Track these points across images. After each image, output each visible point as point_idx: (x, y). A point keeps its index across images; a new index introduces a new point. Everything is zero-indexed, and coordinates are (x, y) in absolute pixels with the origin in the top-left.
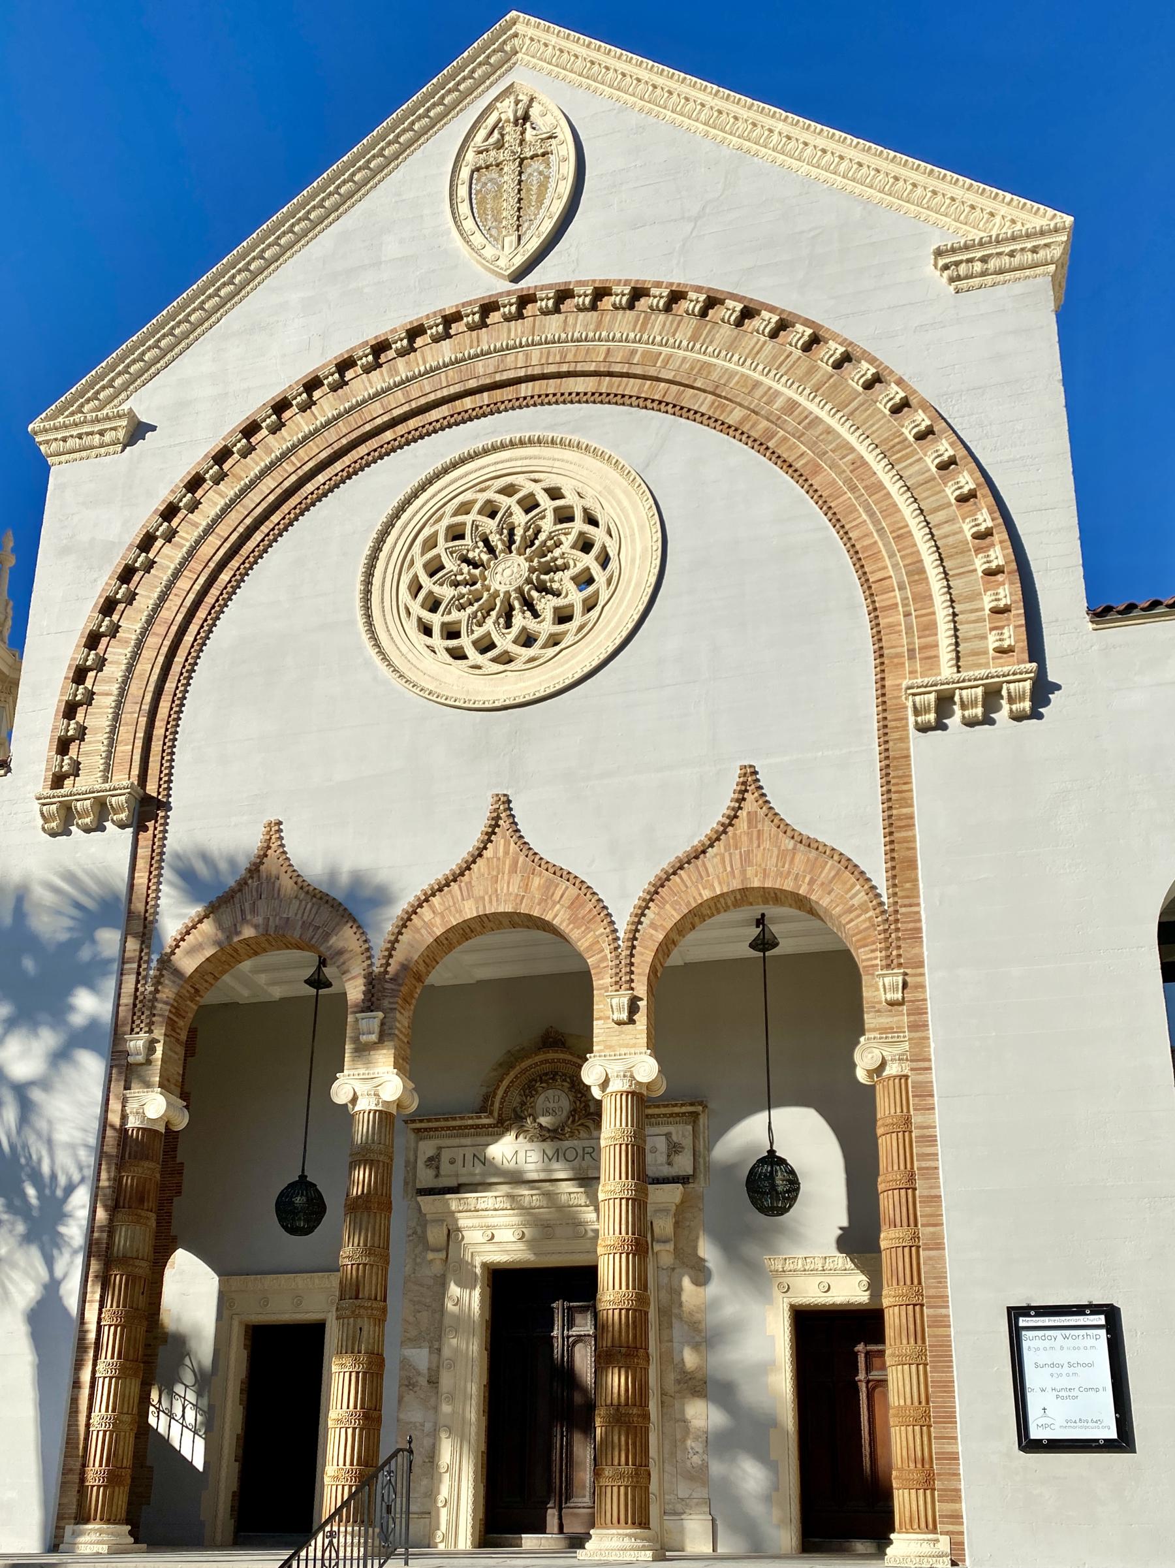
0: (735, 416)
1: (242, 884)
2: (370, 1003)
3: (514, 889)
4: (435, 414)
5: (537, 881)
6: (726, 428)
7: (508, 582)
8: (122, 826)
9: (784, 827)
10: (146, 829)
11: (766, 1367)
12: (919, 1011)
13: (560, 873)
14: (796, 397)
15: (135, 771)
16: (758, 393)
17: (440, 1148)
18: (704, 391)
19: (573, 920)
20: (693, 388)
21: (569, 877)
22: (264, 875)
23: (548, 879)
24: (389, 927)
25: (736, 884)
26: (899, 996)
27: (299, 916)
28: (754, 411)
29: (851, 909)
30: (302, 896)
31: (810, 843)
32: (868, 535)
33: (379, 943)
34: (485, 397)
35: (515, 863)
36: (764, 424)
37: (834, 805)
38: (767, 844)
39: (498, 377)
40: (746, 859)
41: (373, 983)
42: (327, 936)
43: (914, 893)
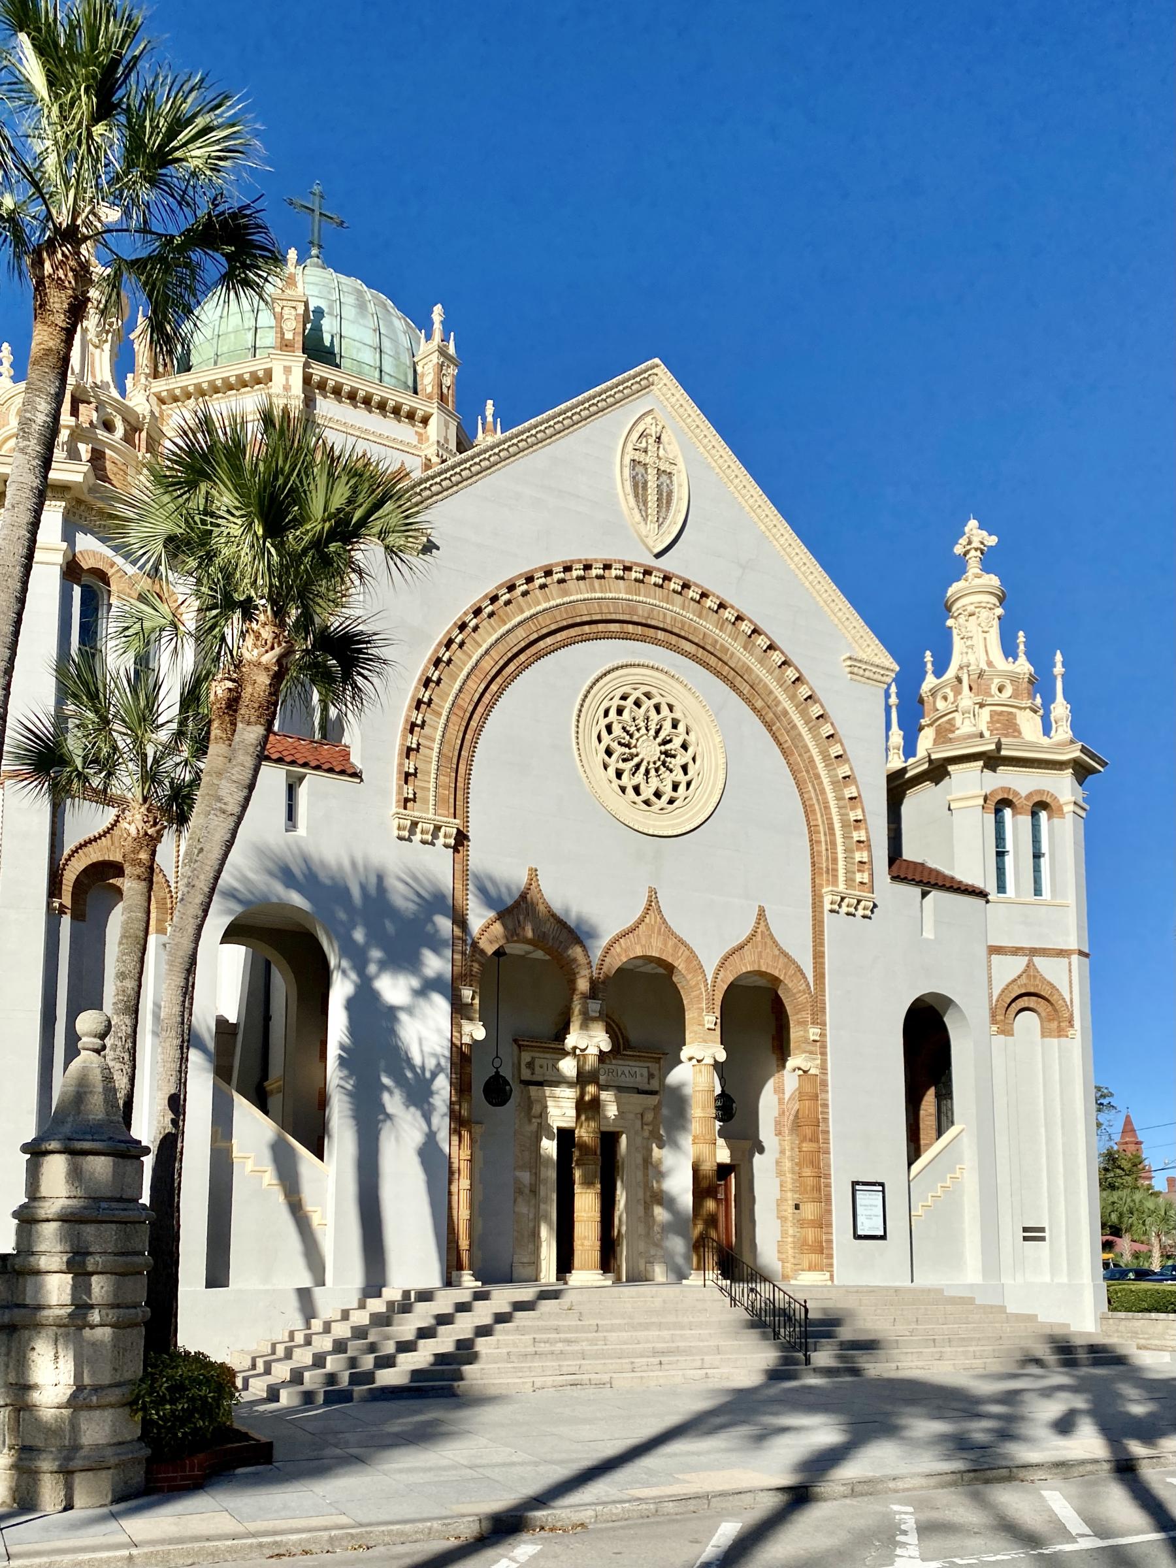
1: (517, 904)
2: (594, 992)
3: (660, 945)
5: (670, 943)
6: (754, 709)
7: (644, 755)
8: (446, 846)
9: (775, 942)
10: (458, 852)
12: (824, 1046)
13: (681, 941)
16: (772, 697)
17: (533, 1058)
19: (687, 969)
21: (687, 946)
25: (756, 968)
29: (800, 991)
31: (786, 955)
32: (811, 799)
40: (760, 956)
41: (593, 983)
42: (567, 948)
43: (823, 990)
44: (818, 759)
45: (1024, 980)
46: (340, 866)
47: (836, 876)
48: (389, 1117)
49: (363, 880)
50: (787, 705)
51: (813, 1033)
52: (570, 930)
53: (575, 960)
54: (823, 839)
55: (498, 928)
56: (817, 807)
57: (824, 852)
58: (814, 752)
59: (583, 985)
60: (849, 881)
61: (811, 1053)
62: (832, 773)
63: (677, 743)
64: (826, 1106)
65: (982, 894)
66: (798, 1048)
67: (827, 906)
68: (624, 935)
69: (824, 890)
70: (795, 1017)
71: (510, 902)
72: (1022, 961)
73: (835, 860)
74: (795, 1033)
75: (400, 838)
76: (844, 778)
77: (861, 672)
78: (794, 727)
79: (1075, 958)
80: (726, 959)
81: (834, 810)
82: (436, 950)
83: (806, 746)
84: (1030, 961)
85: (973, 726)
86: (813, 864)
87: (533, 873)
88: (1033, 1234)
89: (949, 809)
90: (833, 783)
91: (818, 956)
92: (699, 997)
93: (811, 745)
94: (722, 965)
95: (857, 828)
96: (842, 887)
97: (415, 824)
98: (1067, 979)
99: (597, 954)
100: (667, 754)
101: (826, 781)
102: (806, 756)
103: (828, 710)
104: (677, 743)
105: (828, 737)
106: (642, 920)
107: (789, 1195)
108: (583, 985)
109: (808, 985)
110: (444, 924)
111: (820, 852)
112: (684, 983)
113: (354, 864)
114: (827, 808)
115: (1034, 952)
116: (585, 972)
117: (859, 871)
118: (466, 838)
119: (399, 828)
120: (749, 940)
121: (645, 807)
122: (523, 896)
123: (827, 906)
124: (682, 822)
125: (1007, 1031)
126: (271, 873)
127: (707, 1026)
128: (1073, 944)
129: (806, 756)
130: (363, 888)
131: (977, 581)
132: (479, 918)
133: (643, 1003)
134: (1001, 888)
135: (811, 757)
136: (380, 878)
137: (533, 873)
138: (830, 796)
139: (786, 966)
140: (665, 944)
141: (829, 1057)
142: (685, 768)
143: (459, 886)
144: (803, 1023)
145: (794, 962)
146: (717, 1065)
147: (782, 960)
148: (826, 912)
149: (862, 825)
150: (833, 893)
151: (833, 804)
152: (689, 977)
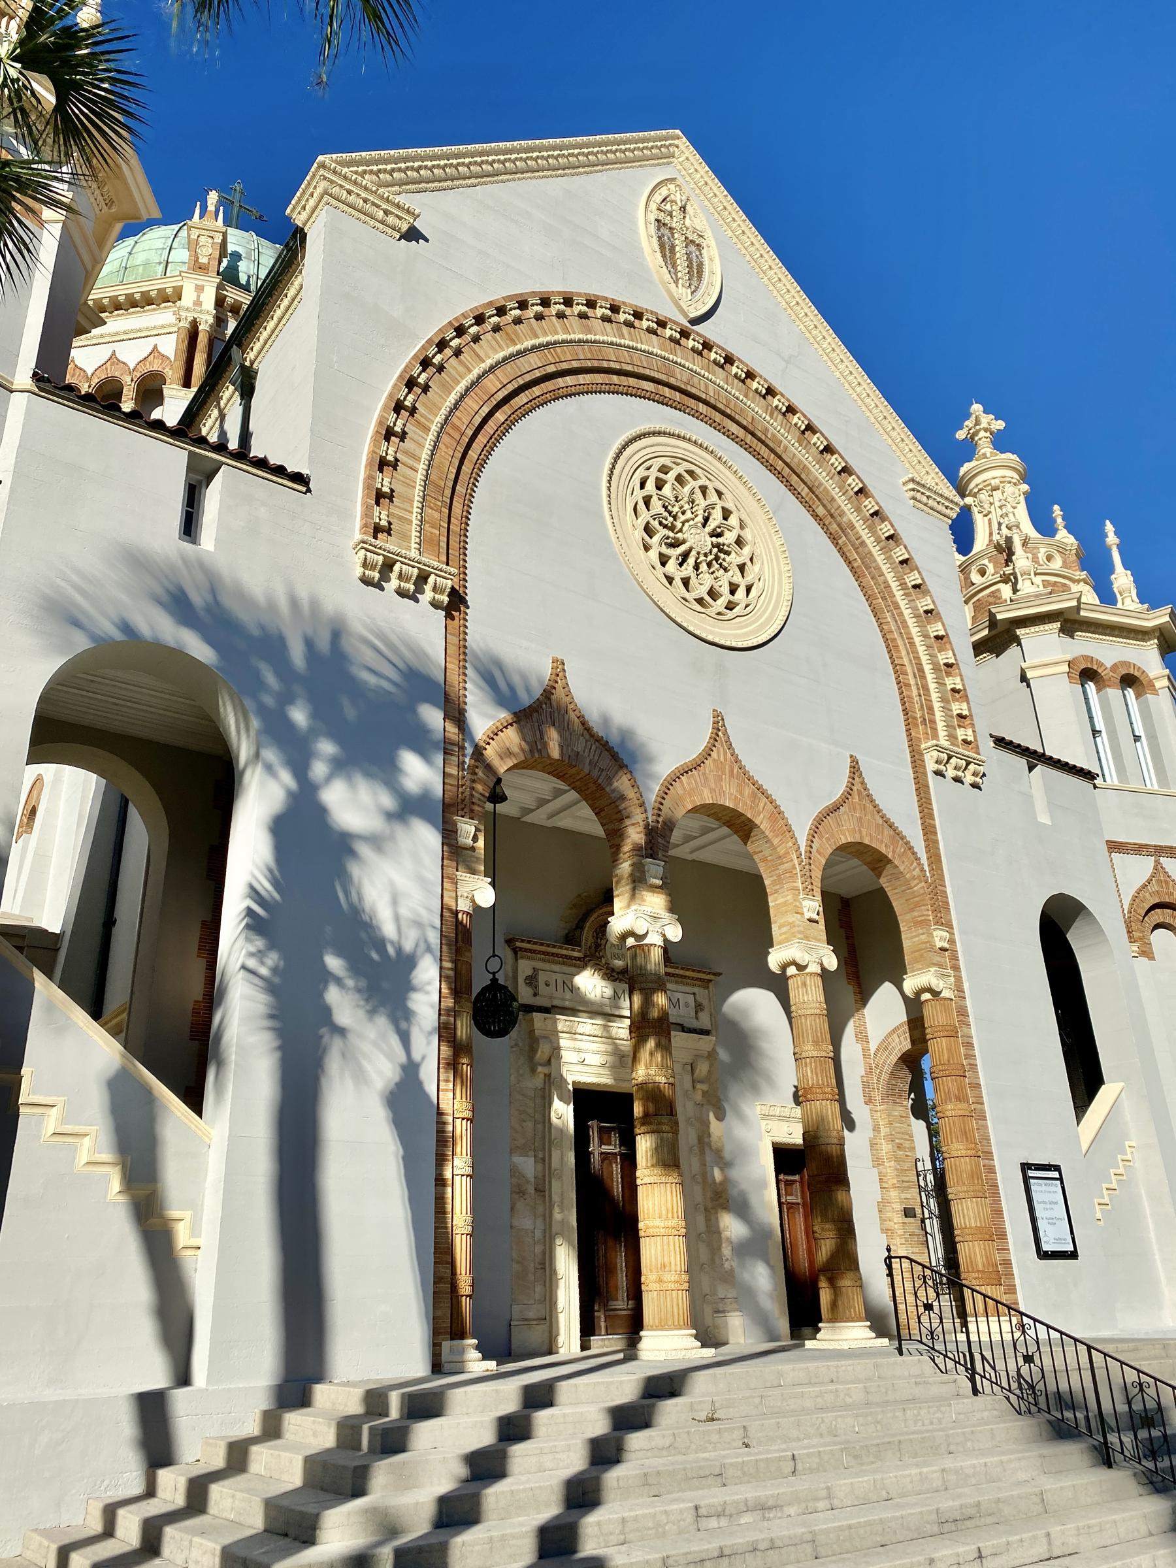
0: (821, 511)
3: (733, 791)
4: (646, 385)
5: (747, 791)
8: (435, 604)
10: (453, 619)
12: (954, 958)
14: (854, 521)
15: (444, 559)
18: (805, 483)
20: (798, 476)
22: (554, 704)
23: (753, 792)
24: (656, 788)
26: (946, 945)
27: (586, 754)
28: (832, 516)
29: (914, 878)
30: (587, 737)
33: (652, 798)
34: (677, 396)
35: (732, 771)
36: (835, 526)
38: (869, 816)
39: (689, 388)
42: (610, 780)
44: (894, 585)
46: (272, 606)
49: (310, 631)
50: (851, 516)
51: (939, 937)
53: (623, 798)
54: (912, 682)
55: (511, 736)
56: (900, 642)
57: (916, 699)
58: (890, 577)
59: (635, 835)
60: (952, 737)
61: (940, 966)
62: (913, 604)
66: (916, 961)
68: (686, 771)
69: (923, 746)
70: (908, 917)
71: (526, 700)
73: (931, 709)
74: (910, 940)
75: (366, 581)
76: (926, 612)
77: (924, 499)
78: (863, 543)
80: (819, 821)
81: (921, 649)
82: (423, 753)
83: (878, 568)
86: (906, 712)
87: (559, 666)
90: (917, 616)
93: (885, 568)
95: (948, 674)
97: (388, 566)
101: (907, 613)
102: (881, 579)
103: (899, 531)
105: (902, 562)
107: (893, 1194)
108: (635, 835)
109: (923, 870)
110: (433, 717)
111: (911, 698)
112: (767, 852)
113: (294, 602)
114: (912, 644)
116: (638, 817)
117: (960, 726)
118: (464, 601)
119: (365, 564)
121: (698, 607)
122: (548, 693)
123: (931, 766)
124: (747, 634)
127: (808, 915)
129: (881, 579)
132: (484, 719)
135: (886, 582)
136: (337, 634)
137: (559, 666)
138: (914, 631)
140: (741, 792)
141: (964, 974)
142: (742, 568)
143: (453, 667)
144: (922, 923)
145: (903, 838)
146: (825, 973)
147: (887, 832)
148: (930, 775)
149: (954, 671)
150: (940, 749)
152: (776, 841)
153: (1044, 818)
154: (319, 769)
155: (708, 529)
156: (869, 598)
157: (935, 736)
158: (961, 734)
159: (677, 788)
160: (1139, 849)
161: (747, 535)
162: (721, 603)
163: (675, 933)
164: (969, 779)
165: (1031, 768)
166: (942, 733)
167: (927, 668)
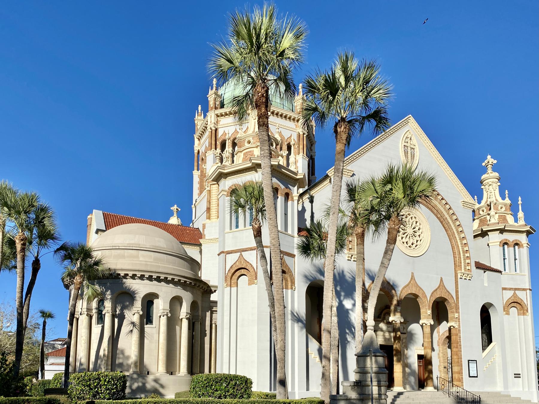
11: (414, 363)
13: (420, 288)
31: (448, 292)
37: (450, 287)
45: (513, 298)
47: (461, 268)
48: (349, 342)
52: (392, 286)
60: (465, 269)
63: (417, 228)
64: (460, 337)
65: (500, 272)
67: (459, 277)
68: (405, 287)
72: (512, 292)
73: (461, 262)
79: (528, 291)
80: (432, 293)
84: (515, 293)
85: (494, 220)
88: (517, 376)
89: (488, 245)
91: (457, 292)
92: (426, 305)
94: (431, 295)
95: (466, 253)
96: (463, 271)
98: (526, 297)
99: (398, 293)
100: (415, 232)
104: (417, 228)
106: (410, 282)
115: (516, 289)
120: (439, 287)
125: (508, 314)
126: (317, 272)
128: (528, 287)
130: (339, 274)
131: (491, 175)
133: (410, 306)
134: (505, 270)
136: (343, 272)
139: (448, 295)
150: (461, 273)
151: (460, 245)
153: (486, 284)
154: (342, 298)
155: (412, 228)
156: (449, 236)
157: (461, 270)
158: (467, 268)
159: (404, 291)
160: (510, 289)
161: (421, 227)
162: (414, 245)
163: (402, 320)
164: (468, 278)
165: (485, 272)
166: (463, 268)
167: (461, 252)
